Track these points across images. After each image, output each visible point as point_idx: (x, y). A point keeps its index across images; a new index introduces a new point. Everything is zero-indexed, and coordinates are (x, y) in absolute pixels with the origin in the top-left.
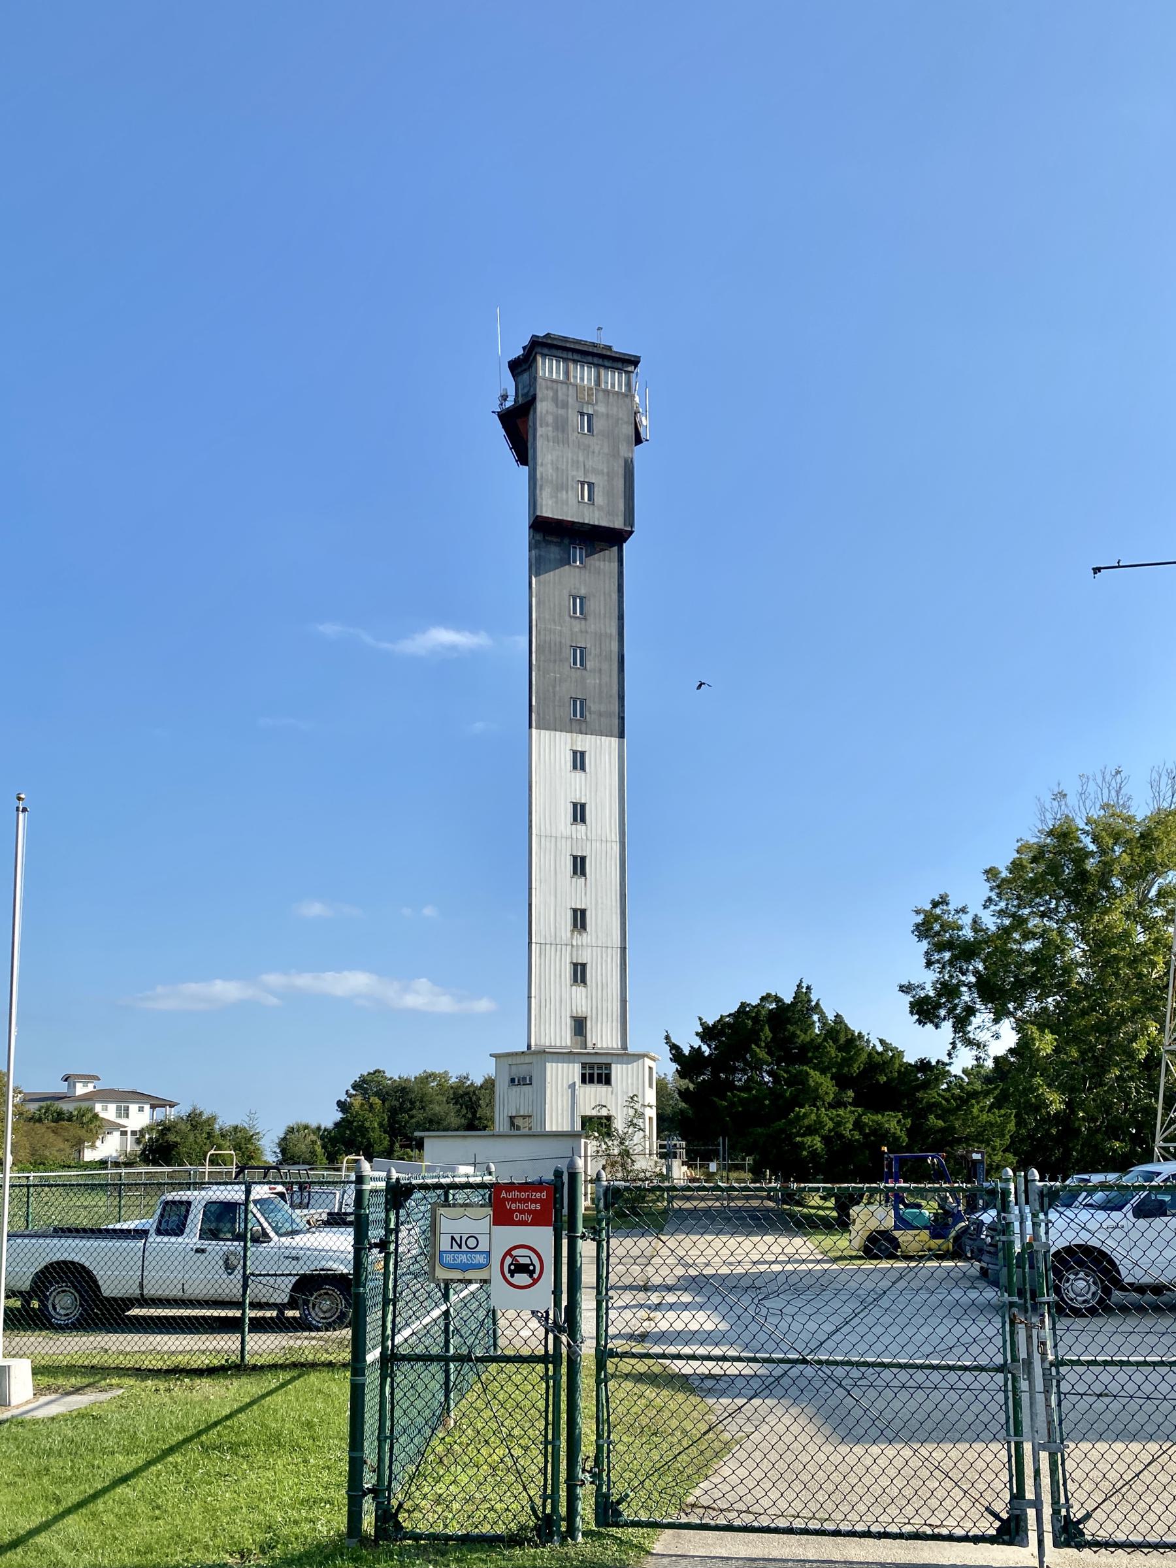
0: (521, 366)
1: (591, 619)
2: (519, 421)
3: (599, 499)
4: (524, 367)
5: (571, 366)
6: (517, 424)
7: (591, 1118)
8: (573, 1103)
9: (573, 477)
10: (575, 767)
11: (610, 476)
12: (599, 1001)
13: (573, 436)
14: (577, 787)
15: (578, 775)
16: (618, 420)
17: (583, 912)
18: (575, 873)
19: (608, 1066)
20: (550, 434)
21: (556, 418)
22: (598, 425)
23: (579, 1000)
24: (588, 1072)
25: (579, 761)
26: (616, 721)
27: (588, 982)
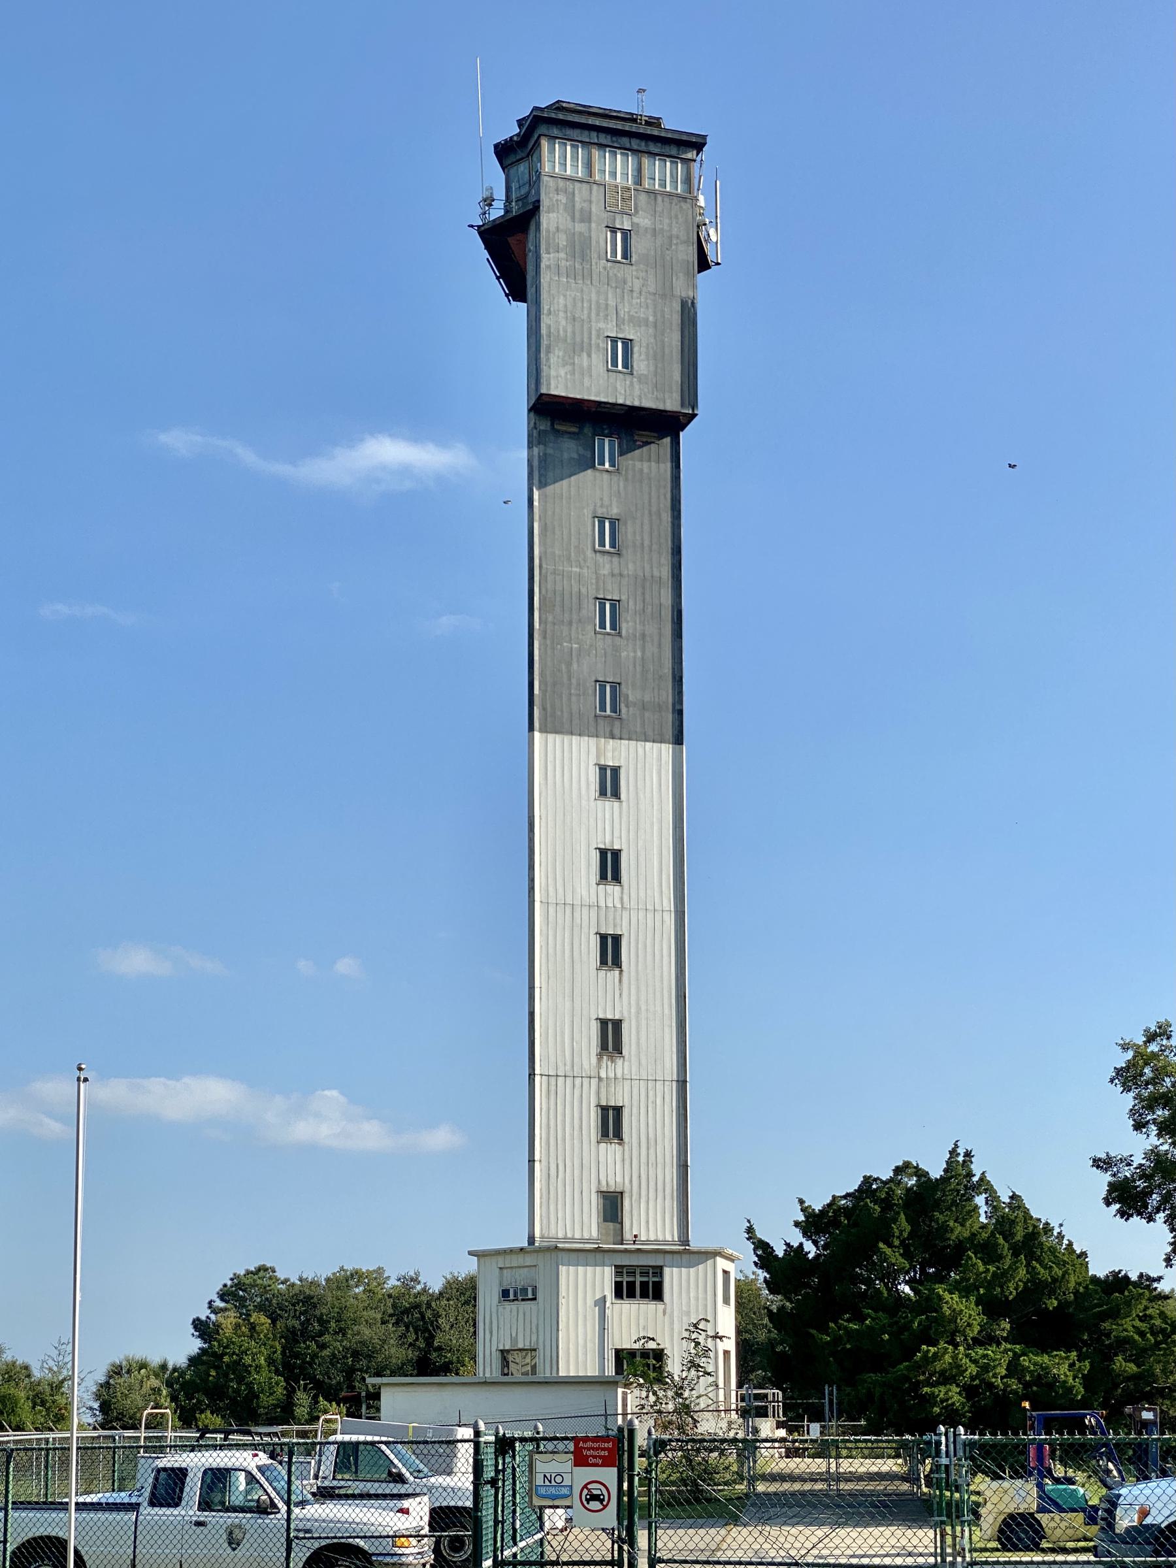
0: (514, 152)
1: (628, 554)
2: (512, 241)
3: (641, 364)
4: (520, 155)
5: (596, 153)
6: (510, 243)
7: (632, 1353)
8: (603, 1329)
9: (599, 331)
10: (603, 793)
12: (640, 1166)
14: (607, 824)
15: (609, 805)
16: (670, 238)
17: (617, 1024)
18: (603, 962)
19: (659, 1271)
20: (563, 263)
21: (572, 236)
22: (639, 246)
23: (611, 1165)
24: (625, 1279)
25: (610, 783)
26: (669, 717)
27: (625, 1136)
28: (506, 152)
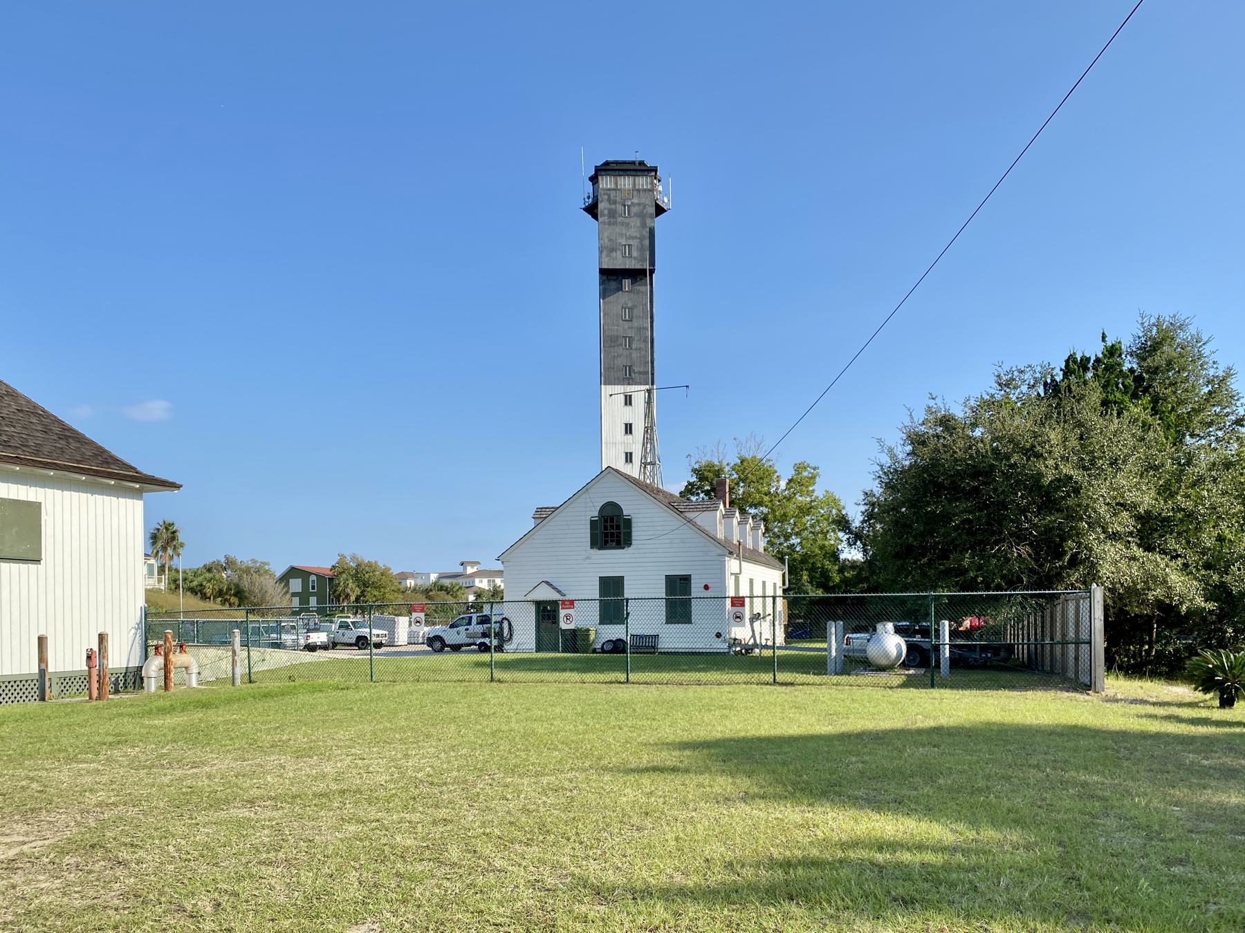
0: (594, 179)
3: (635, 254)
11: (641, 239)
13: (619, 219)
21: (610, 210)
22: (634, 210)
28: (591, 179)
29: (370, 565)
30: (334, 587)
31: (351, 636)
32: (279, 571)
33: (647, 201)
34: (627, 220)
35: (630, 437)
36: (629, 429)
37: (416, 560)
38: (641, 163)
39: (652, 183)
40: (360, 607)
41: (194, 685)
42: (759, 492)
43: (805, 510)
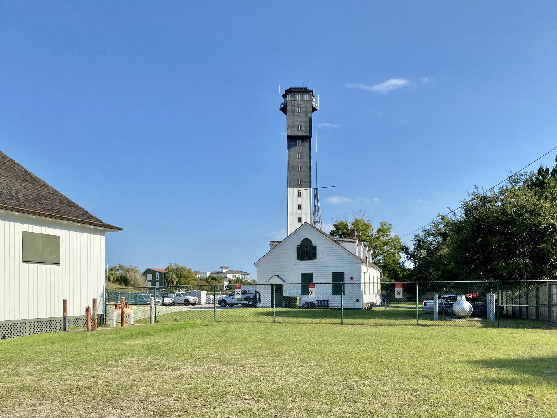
3: (303, 129)
11: (306, 122)
21: (292, 110)
22: (302, 109)
25: (300, 194)
29: (182, 268)
30: (166, 278)
31: (181, 300)
32: (142, 270)
33: (308, 105)
34: (299, 114)
35: (300, 211)
36: (300, 207)
37: (201, 266)
38: (306, 89)
39: (311, 97)
40: (178, 286)
41: (132, 323)
42: (365, 235)
43: (385, 244)
